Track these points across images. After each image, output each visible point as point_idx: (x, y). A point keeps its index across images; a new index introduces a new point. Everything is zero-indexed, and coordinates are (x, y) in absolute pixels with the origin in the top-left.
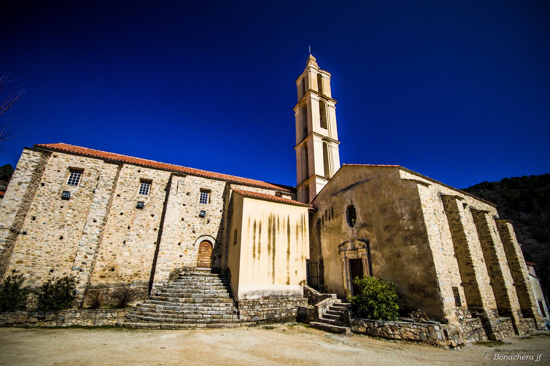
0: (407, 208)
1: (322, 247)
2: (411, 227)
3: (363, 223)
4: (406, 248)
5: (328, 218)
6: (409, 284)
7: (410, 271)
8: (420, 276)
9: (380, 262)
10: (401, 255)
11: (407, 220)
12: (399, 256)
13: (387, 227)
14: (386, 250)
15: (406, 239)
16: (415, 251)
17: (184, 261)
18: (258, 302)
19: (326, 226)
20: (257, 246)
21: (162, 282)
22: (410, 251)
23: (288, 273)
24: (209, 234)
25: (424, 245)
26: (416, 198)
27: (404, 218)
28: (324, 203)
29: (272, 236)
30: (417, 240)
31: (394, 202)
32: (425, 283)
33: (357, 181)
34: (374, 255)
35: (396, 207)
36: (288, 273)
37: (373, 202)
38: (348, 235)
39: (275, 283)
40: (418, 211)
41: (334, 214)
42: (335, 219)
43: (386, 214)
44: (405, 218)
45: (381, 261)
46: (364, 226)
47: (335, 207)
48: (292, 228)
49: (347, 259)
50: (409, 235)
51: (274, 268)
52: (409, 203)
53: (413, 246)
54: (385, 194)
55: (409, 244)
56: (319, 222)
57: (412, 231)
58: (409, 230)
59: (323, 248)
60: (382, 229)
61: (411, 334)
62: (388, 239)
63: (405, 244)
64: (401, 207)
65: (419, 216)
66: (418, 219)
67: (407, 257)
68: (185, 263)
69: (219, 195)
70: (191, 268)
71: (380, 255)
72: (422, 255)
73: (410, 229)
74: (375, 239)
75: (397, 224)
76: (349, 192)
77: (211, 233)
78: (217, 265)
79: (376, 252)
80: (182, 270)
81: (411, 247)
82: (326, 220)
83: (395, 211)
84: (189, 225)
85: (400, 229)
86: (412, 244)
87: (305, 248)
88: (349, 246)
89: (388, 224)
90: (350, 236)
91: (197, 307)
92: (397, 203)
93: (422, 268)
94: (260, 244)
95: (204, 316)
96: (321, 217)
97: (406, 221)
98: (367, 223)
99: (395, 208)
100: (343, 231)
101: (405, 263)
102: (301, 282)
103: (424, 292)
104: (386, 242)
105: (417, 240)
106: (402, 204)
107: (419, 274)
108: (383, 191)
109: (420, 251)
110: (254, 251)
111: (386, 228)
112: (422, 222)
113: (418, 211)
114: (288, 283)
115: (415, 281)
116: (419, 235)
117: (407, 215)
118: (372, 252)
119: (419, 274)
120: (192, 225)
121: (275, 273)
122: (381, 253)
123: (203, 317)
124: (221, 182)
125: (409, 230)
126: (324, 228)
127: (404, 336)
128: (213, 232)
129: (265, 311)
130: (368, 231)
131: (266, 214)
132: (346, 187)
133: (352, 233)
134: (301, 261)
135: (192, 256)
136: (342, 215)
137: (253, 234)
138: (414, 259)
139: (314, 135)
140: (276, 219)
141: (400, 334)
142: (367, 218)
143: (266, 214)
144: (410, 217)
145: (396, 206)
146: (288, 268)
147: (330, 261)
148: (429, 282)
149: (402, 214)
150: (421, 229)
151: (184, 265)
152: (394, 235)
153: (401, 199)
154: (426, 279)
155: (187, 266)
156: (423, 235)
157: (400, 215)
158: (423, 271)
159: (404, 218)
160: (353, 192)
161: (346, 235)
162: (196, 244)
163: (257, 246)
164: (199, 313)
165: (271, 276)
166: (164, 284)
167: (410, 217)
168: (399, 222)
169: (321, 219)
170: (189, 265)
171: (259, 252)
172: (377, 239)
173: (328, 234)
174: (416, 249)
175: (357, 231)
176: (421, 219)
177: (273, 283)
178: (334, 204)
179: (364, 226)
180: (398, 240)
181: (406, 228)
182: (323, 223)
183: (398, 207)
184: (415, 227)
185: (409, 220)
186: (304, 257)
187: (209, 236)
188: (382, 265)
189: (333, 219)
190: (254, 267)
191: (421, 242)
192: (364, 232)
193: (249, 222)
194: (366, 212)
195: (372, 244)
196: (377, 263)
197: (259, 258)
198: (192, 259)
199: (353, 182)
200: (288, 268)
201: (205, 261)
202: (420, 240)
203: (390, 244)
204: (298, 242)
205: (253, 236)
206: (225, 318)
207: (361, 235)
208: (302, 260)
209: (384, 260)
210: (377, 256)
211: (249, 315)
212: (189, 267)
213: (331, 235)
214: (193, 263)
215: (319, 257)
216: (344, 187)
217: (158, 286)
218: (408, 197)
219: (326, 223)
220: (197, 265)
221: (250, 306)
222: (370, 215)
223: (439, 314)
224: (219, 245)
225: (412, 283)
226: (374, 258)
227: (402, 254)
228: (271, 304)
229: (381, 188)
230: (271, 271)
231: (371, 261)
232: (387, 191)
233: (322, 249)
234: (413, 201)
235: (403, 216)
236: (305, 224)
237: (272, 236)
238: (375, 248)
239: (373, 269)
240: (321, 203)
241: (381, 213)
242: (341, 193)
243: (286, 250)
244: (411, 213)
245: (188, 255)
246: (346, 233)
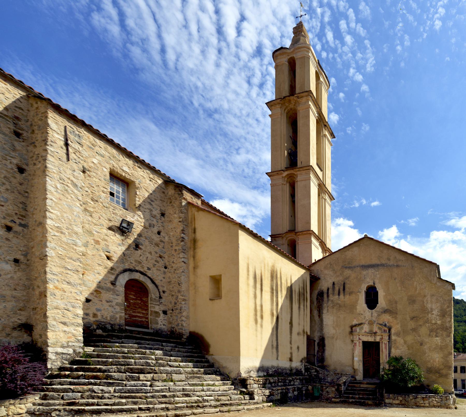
0: (438, 305)
1: (324, 323)
2: (439, 322)
3: (386, 308)
4: (430, 338)
5: (336, 292)
6: (427, 367)
7: (430, 357)
8: (439, 361)
9: (401, 347)
10: (424, 344)
11: (436, 315)
12: (421, 344)
13: (414, 318)
14: (410, 339)
15: (431, 331)
16: (438, 342)
17: (98, 310)
18: (268, 380)
19: (332, 301)
20: (259, 308)
21: (68, 346)
22: (433, 341)
23: (291, 348)
24: (142, 270)
25: (447, 339)
26: (448, 298)
27: (433, 312)
28: (331, 273)
29: (275, 299)
30: (442, 333)
31: (425, 296)
32: (442, 367)
33: (384, 262)
34: (395, 340)
35: (426, 301)
36: (291, 348)
37: (401, 290)
38: (365, 317)
39: (279, 358)
40: (448, 310)
41: (347, 289)
42: (347, 296)
43: (415, 305)
44: (435, 313)
45: (403, 346)
46: (386, 311)
47: (348, 282)
48: (295, 294)
49: (361, 341)
50: (435, 328)
51: (277, 340)
52: (441, 301)
53: (437, 338)
54: (416, 286)
55: (434, 336)
56: (321, 294)
57: (438, 325)
58: (436, 324)
59: (326, 325)
60: (408, 319)
61: (435, 402)
62: (413, 328)
63: (429, 335)
64: (432, 302)
65: (448, 314)
66: (446, 316)
67: (430, 346)
68: (99, 314)
69: (152, 201)
70: (115, 325)
71: (402, 341)
72: (444, 346)
73: (437, 323)
74: (399, 326)
75: (425, 317)
76: (371, 271)
77: (146, 269)
78: (162, 326)
79: (398, 338)
80: (95, 327)
81: (435, 338)
82: (333, 294)
83: (425, 305)
84: (97, 242)
85: (427, 321)
86: (436, 336)
87: (306, 321)
88: (366, 328)
89: (416, 315)
90: (367, 319)
91: (184, 388)
92: (428, 298)
93: (442, 355)
94: (262, 306)
95: (205, 398)
96: (325, 289)
97: (435, 316)
98: (391, 309)
99: (425, 302)
100: (358, 311)
101: (427, 351)
102: (303, 359)
103: (439, 373)
104: (411, 331)
105: (442, 333)
106: (433, 300)
107: (437, 360)
108: (415, 283)
109: (442, 343)
110: (256, 315)
111: (412, 318)
112: (449, 319)
113: (448, 310)
114: (291, 360)
115: (432, 365)
116: (444, 329)
117: (437, 310)
118: (393, 337)
119: (437, 360)
120: (103, 243)
121: (279, 347)
122: (404, 340)
123: (203, 400)
124: (156, 178)
125: (436, 324)
126: (330, 302)
127: (431, 404)
128: (149, 269)
129: (279, 390)
130: (391, 317)
131: (268, 266)
132: (367, 264)
133: (370, 316)
134: (302, 336)
135: (114, 304)
136: (358, 294)
137: (254, 290)
138: (435, 348)
139: (311, 173)
140: (279, 276)
141: (429, 403)
142: (392, 305)
143: (268, 266)
144: (439, 313)
145: (427, 301)
146: (291, 343)
147: (336, 340)
148: (445, 367)
149: (432, 309)
150: (448, 325)
151: (99, 318)
152: (420, 325)
153: (433, 295)
154: (443, 364)
155: (105, 321)
156: (448, 330)
157: (430, 310)
158: (442, 358)
159: (433, 312)
160: (378, 273)
161: (362, 316)
162: (117, 283)
163: (259, 308)
164: (192, 395)
165: (275, 350)
166: (74, 351)
167: (439, 313)
168: (428, 315)
169: (325, 290)
170: (109, 319)
171: (262, 317)
172: (401, 327)
173: (335, 311)
174: (440, 341)
175: (378, 315)
176: (449, 317)
177: (277, 359)
178: (348, 278)
179: (386, 311)
180: (424, 330)
181: (434, 322)
182: (328, 296)
183: (429, 301)
184: (442, 322)
185: (438, 315)
186: (305, 331)
187: (142, 273)
188: (402, 350)
189: (344, 295)
190: (257, 336)
191: (445, 336)
192: (386, 318)
193: (248, 271)
194: (392, 298)
195: (395, 331)
196: (397, 348)
197: (262, 326)
198: (113, 310)
199: (378, 262)
200: (291, 343)
201: (139, 317)
202: (445, 334)
203: (414, 333)
204: (300, 313)
205: (254, 293)
206: (235, 400)
207: (382, 319)
208: (304, 336)
209: (405, 346)
210: (398, 342)
211: (264, 395)
212: (110, 324)
213: (339, 313)
214: (118, 316)
215: (319, 334)
216: (363, 263)
217: (63, 353)
218: (440, 295)
219: (334, 298)
220: (125, 321)
221: (260, 384)
222: (396, 303)
223: (448, 388)
224: (162, 293)
225: (430, 366)
226: (395, 343)
227: (425, 343)
228: (281, 382)
229: (413, 279)
230: (275, 344)
231: (391, 346)
232: (419, 284)
233: (324, 326)
234: (445, 300)
235: (432, 311)
236: (307, 292)
237: (275, 299)
238: (398, 334)
239: (392, 353)
240: (326, 272)
241: (409, 303)
242: (359, 268)
243: (289, 321)
244: (441, 310)
245: (104, 302)
246: (362, 314)
